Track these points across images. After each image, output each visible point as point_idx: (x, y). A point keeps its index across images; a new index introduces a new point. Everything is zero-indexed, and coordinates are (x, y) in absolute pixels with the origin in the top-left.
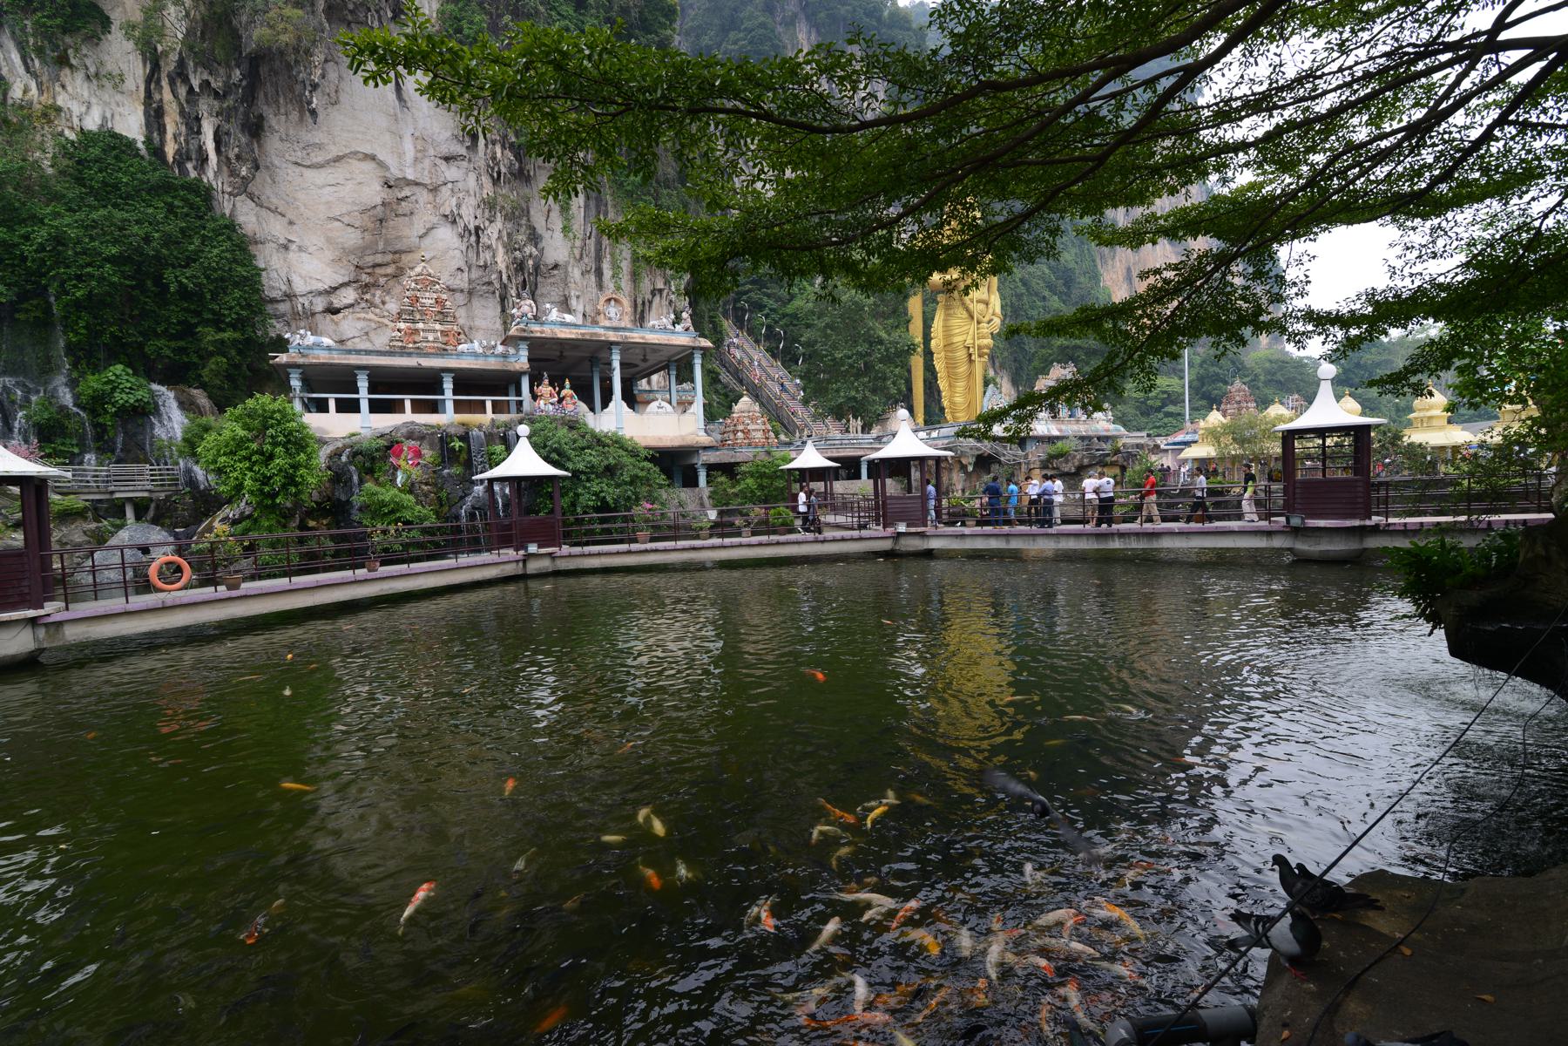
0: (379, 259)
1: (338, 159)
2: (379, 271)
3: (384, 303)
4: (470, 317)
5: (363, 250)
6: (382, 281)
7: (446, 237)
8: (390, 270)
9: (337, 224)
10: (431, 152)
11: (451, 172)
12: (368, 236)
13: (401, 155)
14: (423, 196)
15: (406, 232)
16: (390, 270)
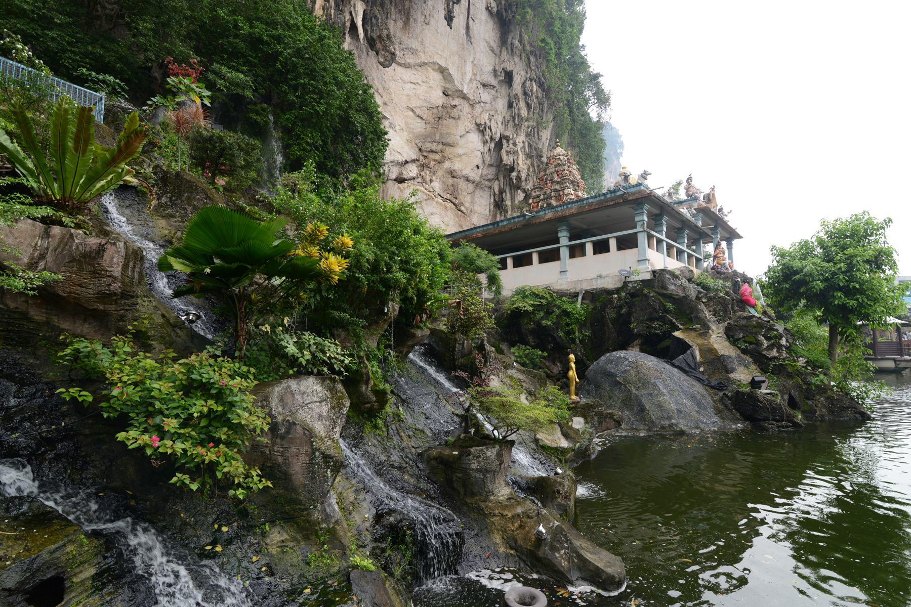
0: (434, 147)
1: (424, 64)
2: (432, 156)
3: (431, 181)
4: (472, 203)
5: (425, 137)
6: (432, 163)
7: (474, 139)
8: (437, 157)
9: (411, 113)
10: (478, 78)
11: (486, 96)
12: (429, 127)
13: (464, 74)
14: (467, 108)
15: (453, 131)
16: (437, 157)
